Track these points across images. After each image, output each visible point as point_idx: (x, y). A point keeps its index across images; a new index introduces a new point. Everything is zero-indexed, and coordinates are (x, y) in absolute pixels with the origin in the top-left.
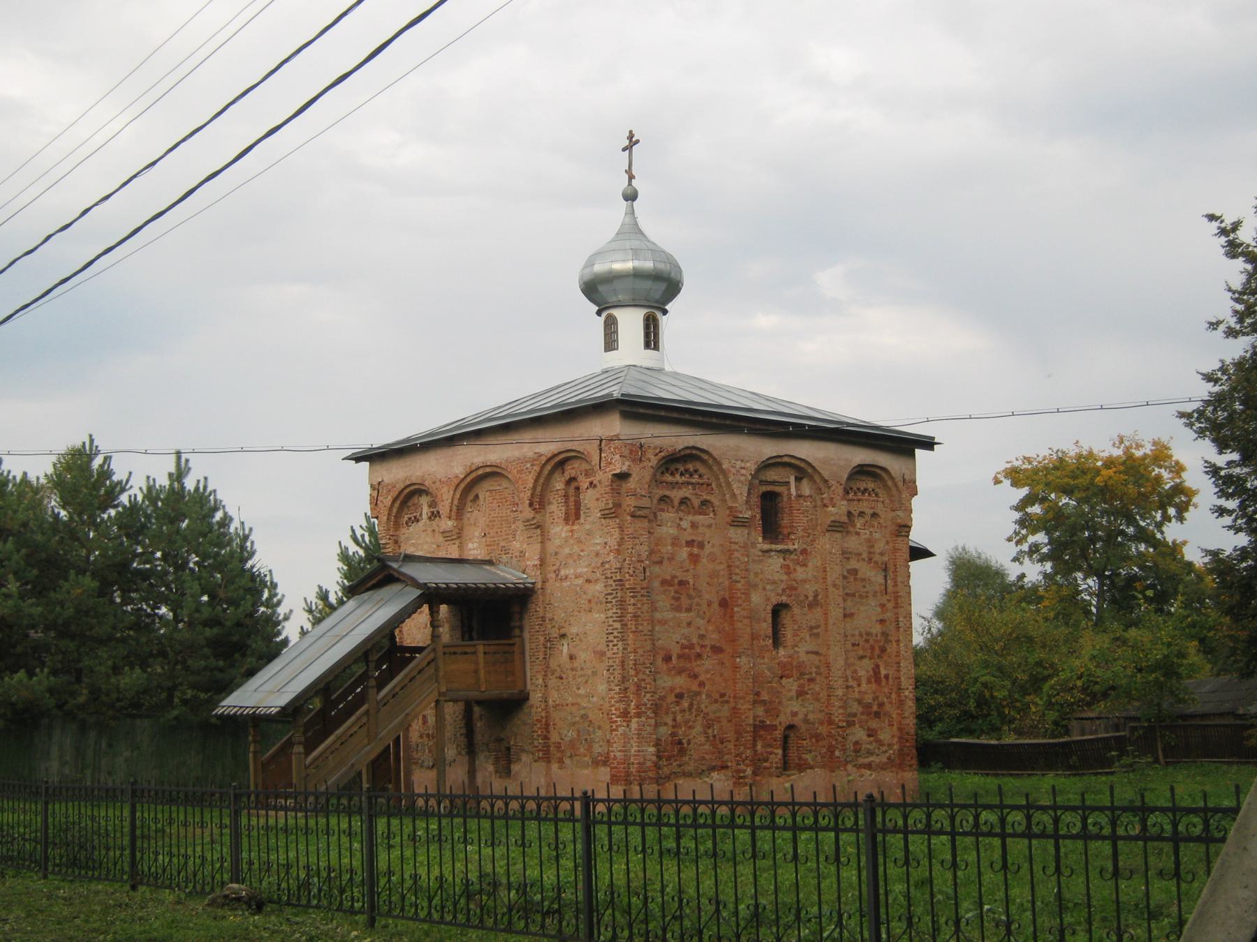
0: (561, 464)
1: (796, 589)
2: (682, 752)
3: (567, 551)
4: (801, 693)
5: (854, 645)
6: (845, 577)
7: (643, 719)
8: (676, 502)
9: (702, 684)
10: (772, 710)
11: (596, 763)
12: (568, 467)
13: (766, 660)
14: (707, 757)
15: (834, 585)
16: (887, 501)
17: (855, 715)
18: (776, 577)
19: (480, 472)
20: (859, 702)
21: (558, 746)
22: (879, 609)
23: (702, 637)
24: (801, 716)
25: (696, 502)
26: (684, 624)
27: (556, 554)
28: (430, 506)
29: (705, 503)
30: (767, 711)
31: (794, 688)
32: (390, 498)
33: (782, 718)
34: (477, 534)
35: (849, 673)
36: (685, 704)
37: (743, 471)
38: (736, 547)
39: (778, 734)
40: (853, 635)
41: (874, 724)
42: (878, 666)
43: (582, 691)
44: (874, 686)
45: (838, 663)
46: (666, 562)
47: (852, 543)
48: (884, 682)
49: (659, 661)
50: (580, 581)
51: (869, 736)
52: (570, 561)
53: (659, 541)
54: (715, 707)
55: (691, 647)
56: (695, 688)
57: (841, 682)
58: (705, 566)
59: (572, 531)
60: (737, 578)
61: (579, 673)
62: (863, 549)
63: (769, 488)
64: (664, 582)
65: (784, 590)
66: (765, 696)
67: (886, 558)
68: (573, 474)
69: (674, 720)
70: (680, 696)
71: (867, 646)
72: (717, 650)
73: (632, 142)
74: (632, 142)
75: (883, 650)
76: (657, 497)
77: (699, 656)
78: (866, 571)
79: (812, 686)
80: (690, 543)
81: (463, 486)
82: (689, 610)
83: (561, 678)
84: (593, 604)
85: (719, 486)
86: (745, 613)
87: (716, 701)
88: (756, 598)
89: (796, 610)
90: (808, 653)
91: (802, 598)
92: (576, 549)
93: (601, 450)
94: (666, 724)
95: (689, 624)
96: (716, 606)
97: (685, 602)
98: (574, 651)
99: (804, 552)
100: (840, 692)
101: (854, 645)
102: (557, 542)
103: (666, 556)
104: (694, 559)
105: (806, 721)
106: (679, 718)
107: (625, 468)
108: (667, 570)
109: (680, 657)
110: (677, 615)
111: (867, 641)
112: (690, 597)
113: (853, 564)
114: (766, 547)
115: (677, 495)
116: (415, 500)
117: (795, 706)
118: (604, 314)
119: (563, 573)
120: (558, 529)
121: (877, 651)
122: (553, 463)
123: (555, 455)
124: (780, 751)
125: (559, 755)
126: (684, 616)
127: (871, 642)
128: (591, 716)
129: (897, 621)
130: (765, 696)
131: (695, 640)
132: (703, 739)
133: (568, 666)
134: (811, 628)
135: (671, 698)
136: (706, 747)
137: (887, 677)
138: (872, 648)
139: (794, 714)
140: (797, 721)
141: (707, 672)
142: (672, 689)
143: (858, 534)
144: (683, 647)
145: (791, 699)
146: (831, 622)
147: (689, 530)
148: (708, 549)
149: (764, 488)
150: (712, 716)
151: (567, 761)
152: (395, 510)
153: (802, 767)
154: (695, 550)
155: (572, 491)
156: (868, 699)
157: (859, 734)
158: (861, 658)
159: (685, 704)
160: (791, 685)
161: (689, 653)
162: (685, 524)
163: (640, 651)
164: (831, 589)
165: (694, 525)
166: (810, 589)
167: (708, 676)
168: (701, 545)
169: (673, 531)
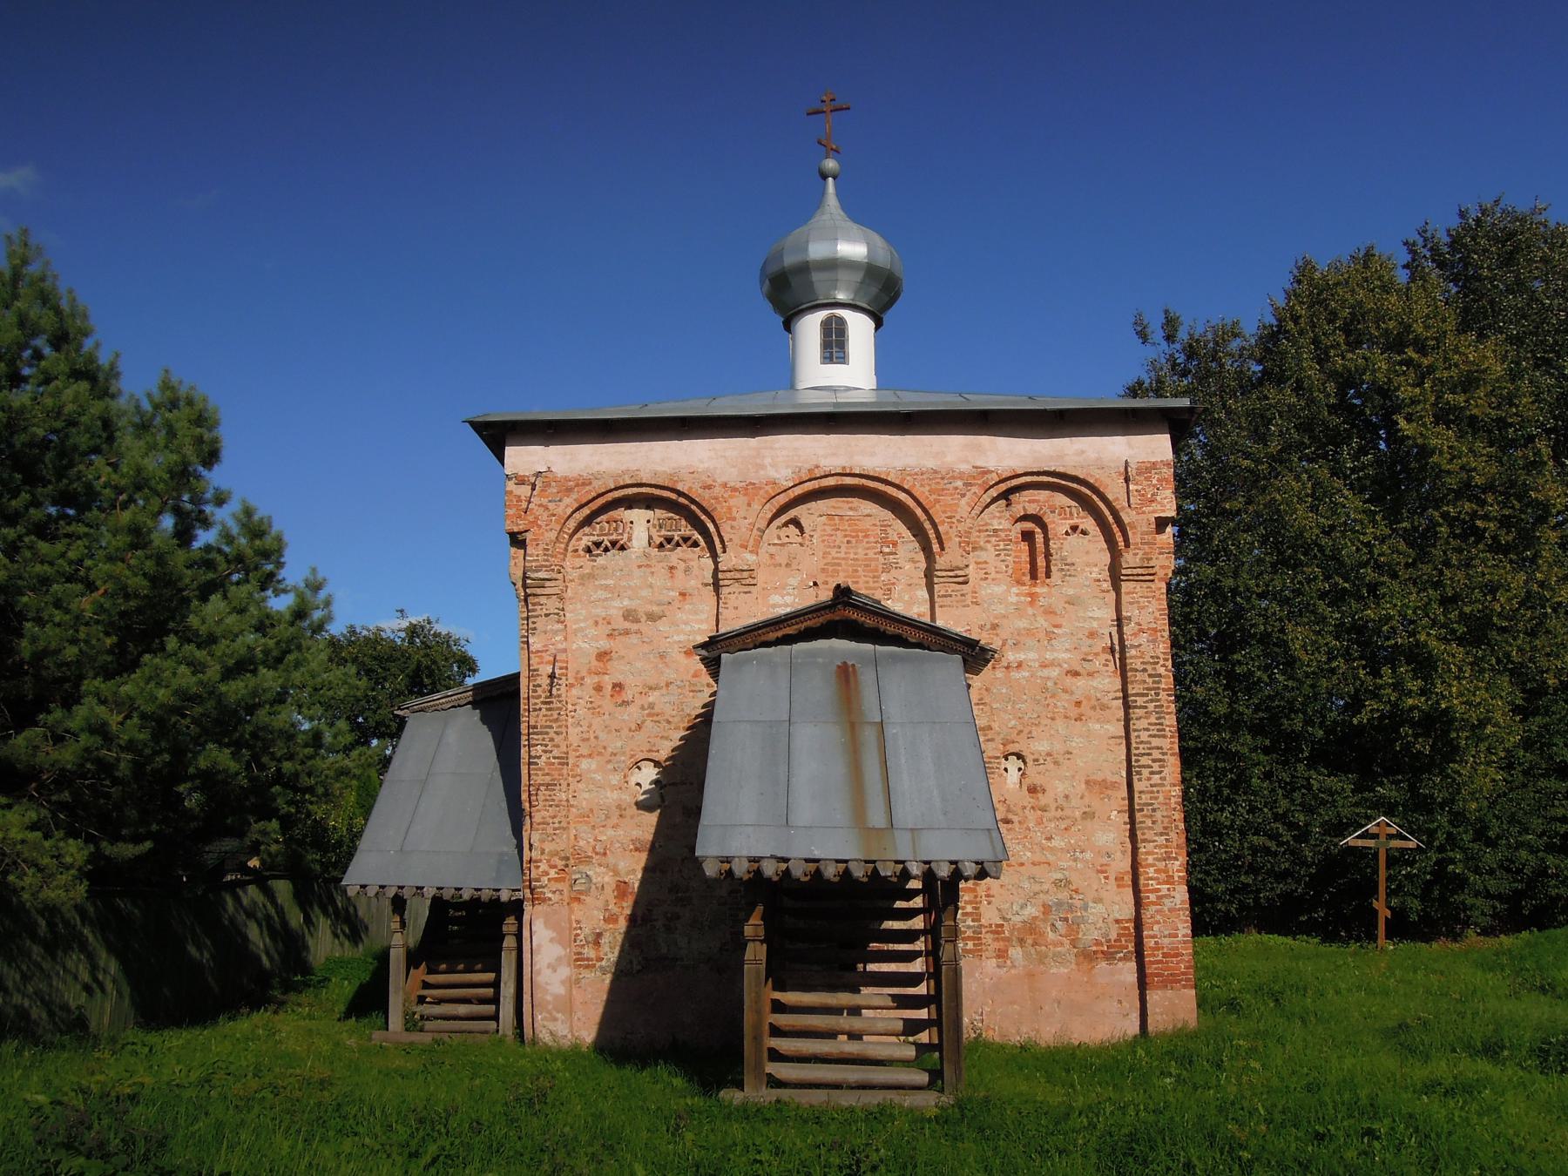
0: (1006, 495)
3: (1022, 624)
11: (1088, 957)
12: (1014, 497)
19: (831, 482)
21: (997, 931)
27: (994, 627)
32: (569, 502)
34: (794, 582)
43: (1057, 842)
50: (1054, 673)
52: (1030, 642)
59: (1033, 596)
61: (1052, 813)
68: (1032, 509)
81: (783, 499)
84: (1085, 708)
92: (1042, 622)
93: (1127, 480)
102: (1001, 609)
120: (998, 590)
122: (1003, 487)
125: (997, 945)
128: (1077, 882)
133: (1027, 800)
151: (1016, 952)
152: (572, 524)
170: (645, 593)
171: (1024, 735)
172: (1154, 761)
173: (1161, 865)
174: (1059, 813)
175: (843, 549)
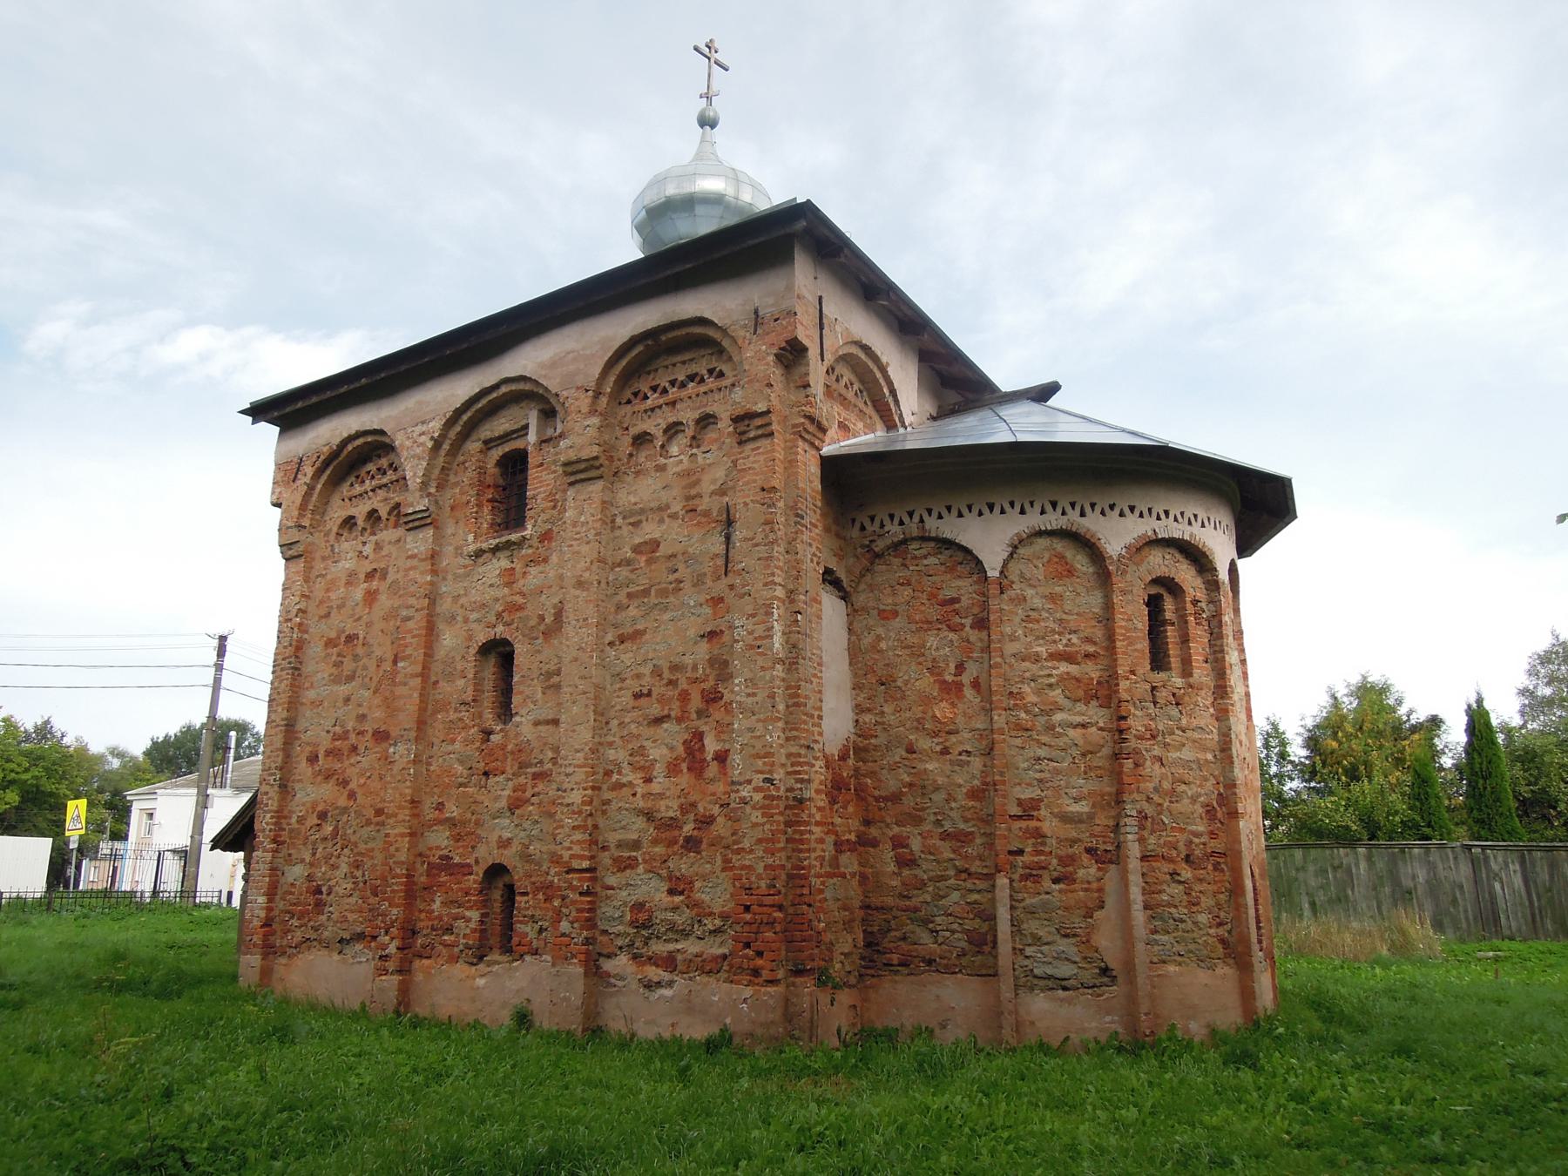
1: (520, 608)
2: (320, 905)
4: (515, 806)
10: (463, 832)
13: (457, 746)
14: (351, 917)
17: (636, 845)
20: (649, 815)
22: (707, 610)
30: (458, 838)
33: (481, 851)
36: (328, 829)
39: (473, 881)
40: (638, 676)
41: (684, 865)
42: (699, 736)
44: (685, 779)
47: (641, 490)
48: (713, 769)
51: (671, 892)
56: (342, 802)
63: (507, 448)
65: (499, 616)
71: (672, 693)
79: (540, 787)
87: (369, 823)
90: (537, 723)
94: (303, 861)
95: (347, 700)
97: (348, 665)
101: (637, 696)
103: (334, 604)
105: (526, 857)
109: (328, 753)
110: (336, 688)
111: (672, 683)
112: (356, 658)
115: (360, 510)
117: (504, 827)
121: (696, 702)
126: (343, 689)
127: (683, 684)
131: (349, 727)
132: (350, 886)
134: (549, 675)
136: (352, 900)
139: (504, 844)
140: (508, 857)
142: (314, 805)
144: (336, 738)
145: (498, 814)
149: (496, 453)
150: (362, 847)
156: (669, 808)
157: (654, 891)
158: (658, 721)
160: (501, 789)
162: (368, 550)
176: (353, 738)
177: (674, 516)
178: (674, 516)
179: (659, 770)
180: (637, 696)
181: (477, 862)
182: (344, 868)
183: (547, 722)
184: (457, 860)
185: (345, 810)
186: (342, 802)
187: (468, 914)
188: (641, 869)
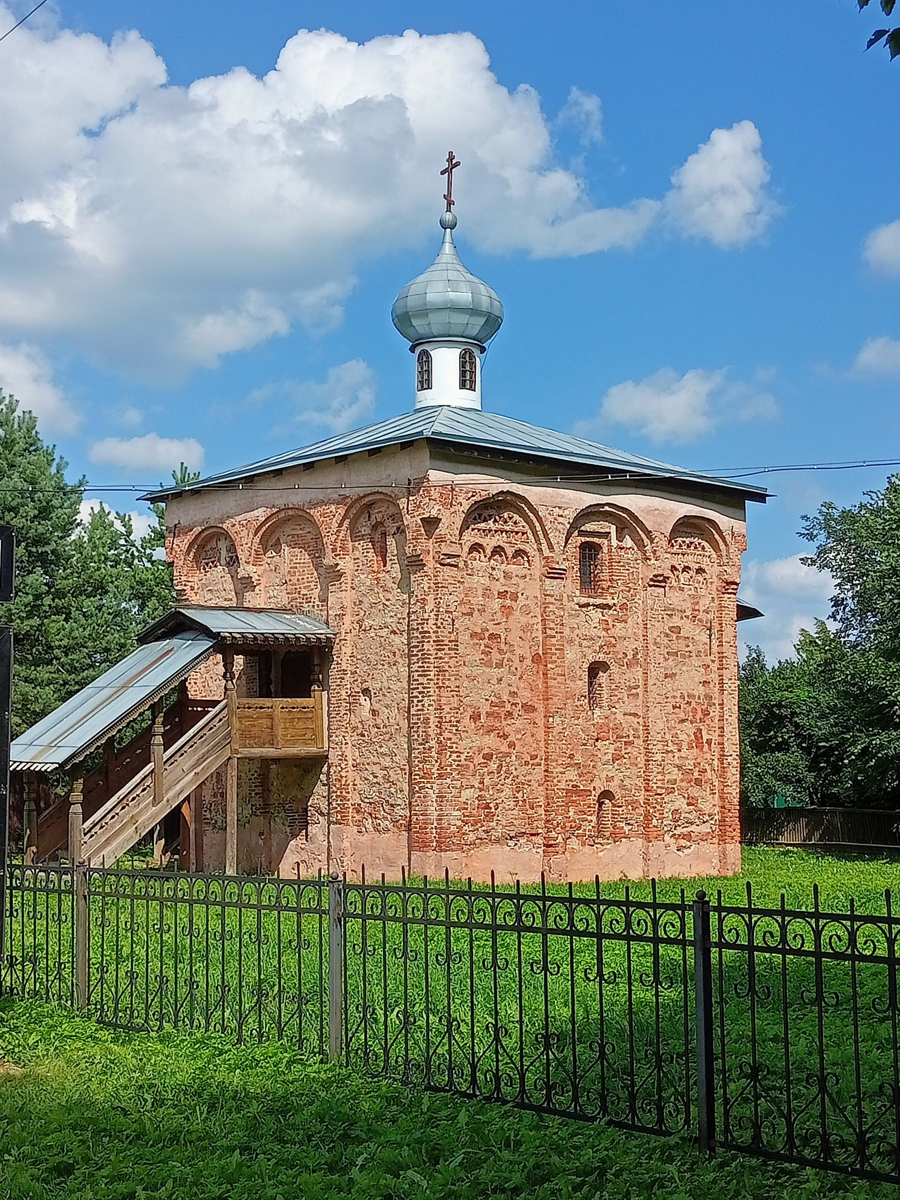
2: (490, 816)
5: (674, 707)
6: (667, 635)
7: (449, 781)
8: (489, 552)
9: (512, 745)
15: (655, 643)
16: (714, 556)
18: (594, 633)
20: (679, 767)
23: (514, 694)
24: (617, 782)
25: (510, 551)
26: (494, 681)
28: (228, 551)
29: (519, 553)
31: (611, 751)
33: (597, 783)
35: (668, 737)
36: (494, 766)
37: (561, 520)
38: (552, 600)
39: (593, 799)
40: (674, 697)
41: (695, 791)
45: (658, 726)
46: (476, 613)
47: (675, 598)
49: (466, 721)
51: (688, 804)
53: (469, 592)
54: (524, 770)
55: (501, 704)
56: (504, 748)
57: (660, 746)
58: (518, 619)
60: (553, 633)
62: (687, 605)
64: (473, 635)
65: (601, 647)
66: (579, 759)
67: (710, 616)
69: (482, 783)
70: (488, 757)
72: (529, 708)
73: (452, 164)
74: (452, 164)
75: (706, 713)
76: (469, 544)
77: (509, 714)
78: (688, 628)
80: (502, 595)
82: (500, 665)
83: (363, 736)
85: (535, 534)
86: (559, 670)
87: (527, 763)
88: (571, 654)
89: (614, 668)
91: (621, 656)
96: (528, 661)
97: (496, 656)
98: (376, 706)
99: (624, 607)
100: (658, 757)
104: (507, 611)
105: (623, 787)
106: (487, 781)
107: (434, 513)
108: (478, 622)
111: (689, 703)
113: (676, 621)
114: (584, 600)
115: (489, 543)
116: (213, 544)
117: (610, 770)
118: (418, 350)
119: (367, 623)
121: (699, 715)
123: (361, 498)
124: (594, 818)
125: (358, 817)
126: (496, 672)
127: (693, 704)
129: (721, 683)
130: (579, 759)
131: (505, 698)
134: (630, 688)
135: (479, 759)
136: (515, 812)
137: (709, 742)
138: (695, 711)
139: (610, 779)
140: (613, 787)
141: (518, 731)
143: (682, 589)
146: (650, 682)
147: (502, 580)
148: (521, 601)
151: (369, 823)
153: (617, 837)
154: (508, 602)
155: (377, 536)
158: (683, 721)
159: (494, 766)
160: (607, 749)
161: (500, 711)
163: (447, 709)
164: (651, 647)
165: (507, 576)
166: (630, 646)
167: (519, 736)
168: (515, 598)
169: (486, 581)
170: (223, 593)
171: (371, 677)
172: (420, 693)
173: (421, 766)
174: (384, 730)
175: (299, 557)
176: (508, 707)
177: (687, 617)
178: (687, 617)
179: (685, 746)
180: (674, 707)
181: (595, 789)
182: (507, 792)
183: (630, 714)
184: (582, 788)
185: (508, 755)
186: (504, 748)
187: (589, 818)
188: (676, 794)
